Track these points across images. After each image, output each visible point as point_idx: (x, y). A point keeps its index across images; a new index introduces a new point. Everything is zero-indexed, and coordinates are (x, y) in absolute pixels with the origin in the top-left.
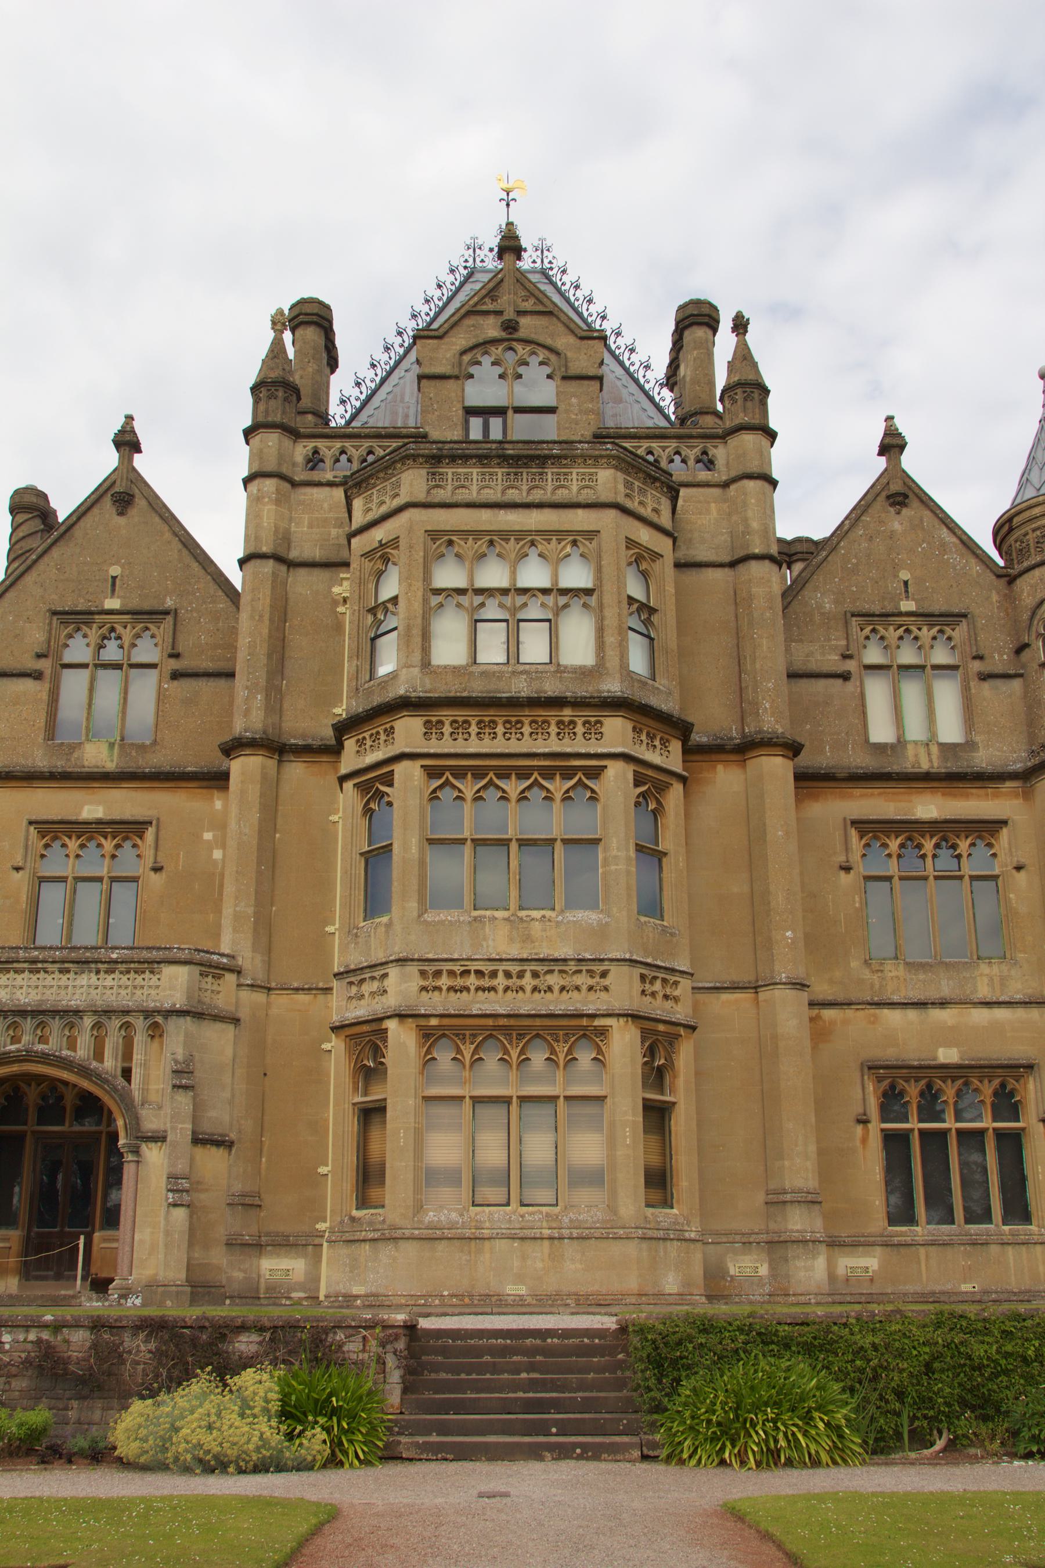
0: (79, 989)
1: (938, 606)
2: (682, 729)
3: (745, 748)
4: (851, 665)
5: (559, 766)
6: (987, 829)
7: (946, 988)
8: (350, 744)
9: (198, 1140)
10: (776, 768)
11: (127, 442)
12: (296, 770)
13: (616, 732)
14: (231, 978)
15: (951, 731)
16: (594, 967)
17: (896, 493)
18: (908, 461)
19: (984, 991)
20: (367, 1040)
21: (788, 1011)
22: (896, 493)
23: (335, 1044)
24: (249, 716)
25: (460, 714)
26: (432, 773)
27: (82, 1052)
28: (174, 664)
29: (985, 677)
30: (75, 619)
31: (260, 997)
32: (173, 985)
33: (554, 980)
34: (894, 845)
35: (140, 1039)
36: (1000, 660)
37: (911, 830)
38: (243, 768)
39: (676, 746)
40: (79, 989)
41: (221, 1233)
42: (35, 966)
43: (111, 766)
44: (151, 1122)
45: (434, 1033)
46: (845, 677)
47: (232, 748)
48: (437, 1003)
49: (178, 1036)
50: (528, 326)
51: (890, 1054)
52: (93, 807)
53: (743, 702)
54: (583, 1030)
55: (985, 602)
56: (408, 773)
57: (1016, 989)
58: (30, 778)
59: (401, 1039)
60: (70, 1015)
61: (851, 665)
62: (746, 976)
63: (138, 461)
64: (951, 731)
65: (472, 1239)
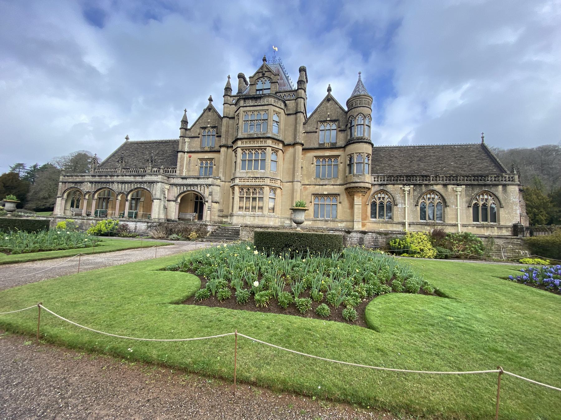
1: (334, 118)
2: (282, 142)
3: (294, 145)
4: (317, 130)
5: (260, 148)
9: (212, 202)
10: (299, 148)
11: (211, 100)
13: (269, 142)
14: (219, 180)
17: (329, 99)
18: (331, 93)
22: (329, 99)
24: (223, 142)
25: (246, 140)
28: (216, 135)
29: (340, 131)
31: (224, 183)
33: (257, 180)
34: (321, 160)
35: (206, 188)
36: (343, 127)
37: (324, 157)
38: (223, 150)
41: (217, 214)
43: (209, 150)
44: (206, 200)
46: (316, 132)
47: (221, 147)
48: (241, 183)
50: (267, 74)
51: (317, 192)
52: (207, 156)
56: (239, 149)
57: (338, 183)
60: (197, 185)
61: (317, 130)
65: (244, 216)
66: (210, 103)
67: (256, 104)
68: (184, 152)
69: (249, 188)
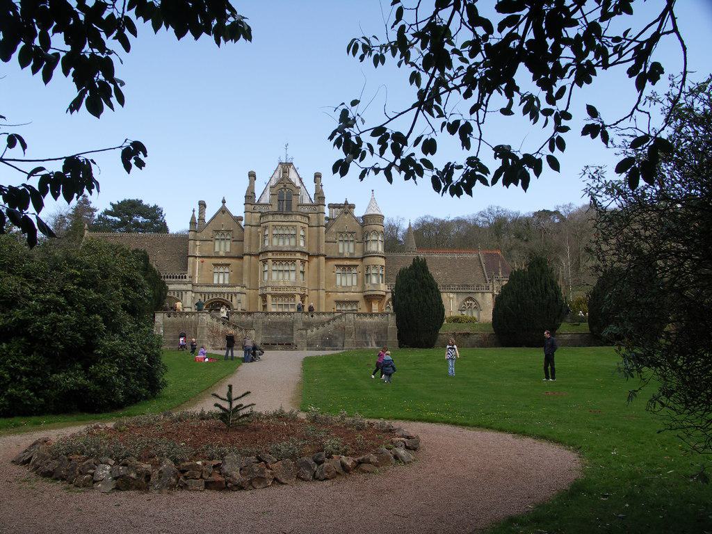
0: (225, 290)
2: (308, 254)
3: (318, 256)
6: (357, 266)
7: (347, 290)
8: (261, 256)
11: (224, 202)
12: (253, 258)
13: (298, 256)
15: (352, 251)
16: (294, 287)
19: (353, 290)
20: (264, 297)
21: (323, 294)
23: (260, 299)
26: (273, 261)
27: (226, 298)
30: (217, 231)
32: (238, 289)
35: (234, 297)
39: (307, 256)
40: (225, 290)
42: (218, 286)
45: (273, 296)
49: (239, 296)
53: (318, 248)
54: (293, 296)
55: (358, 230)
58: (212, 257)
59: (269, 297)
62: (317, 288)
63: (226, 204)
64: (352, 251)
66: (224, 204)
67: (284, 220)
68: (196, 257)
69: (281, 296)
